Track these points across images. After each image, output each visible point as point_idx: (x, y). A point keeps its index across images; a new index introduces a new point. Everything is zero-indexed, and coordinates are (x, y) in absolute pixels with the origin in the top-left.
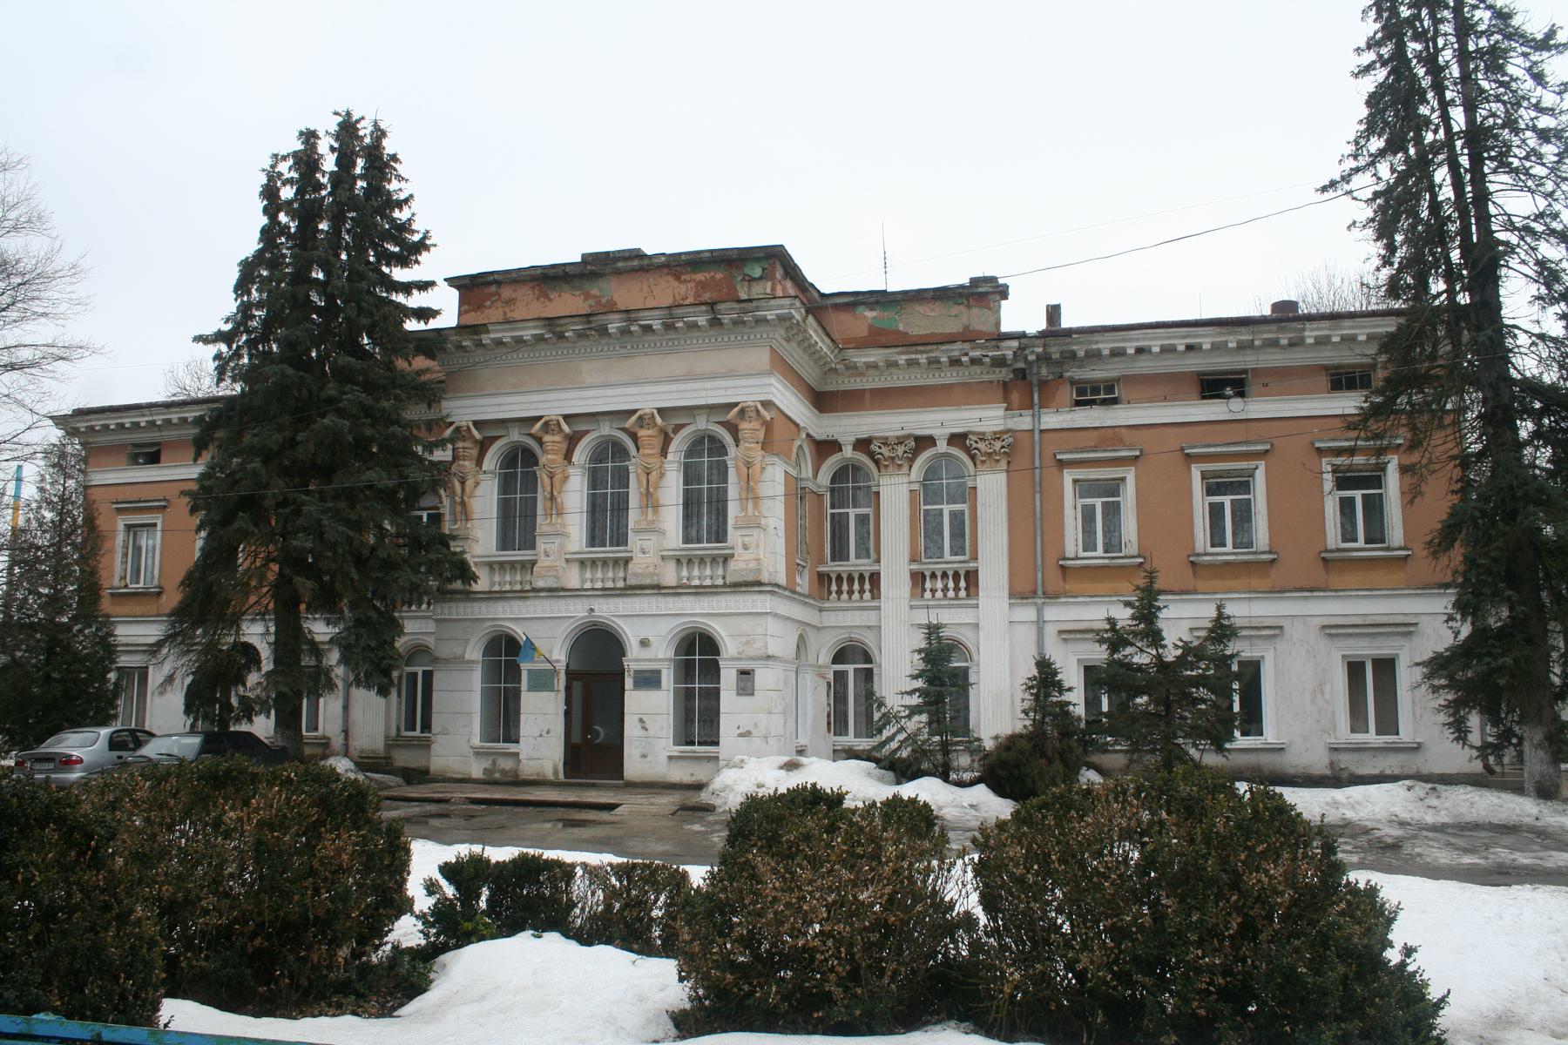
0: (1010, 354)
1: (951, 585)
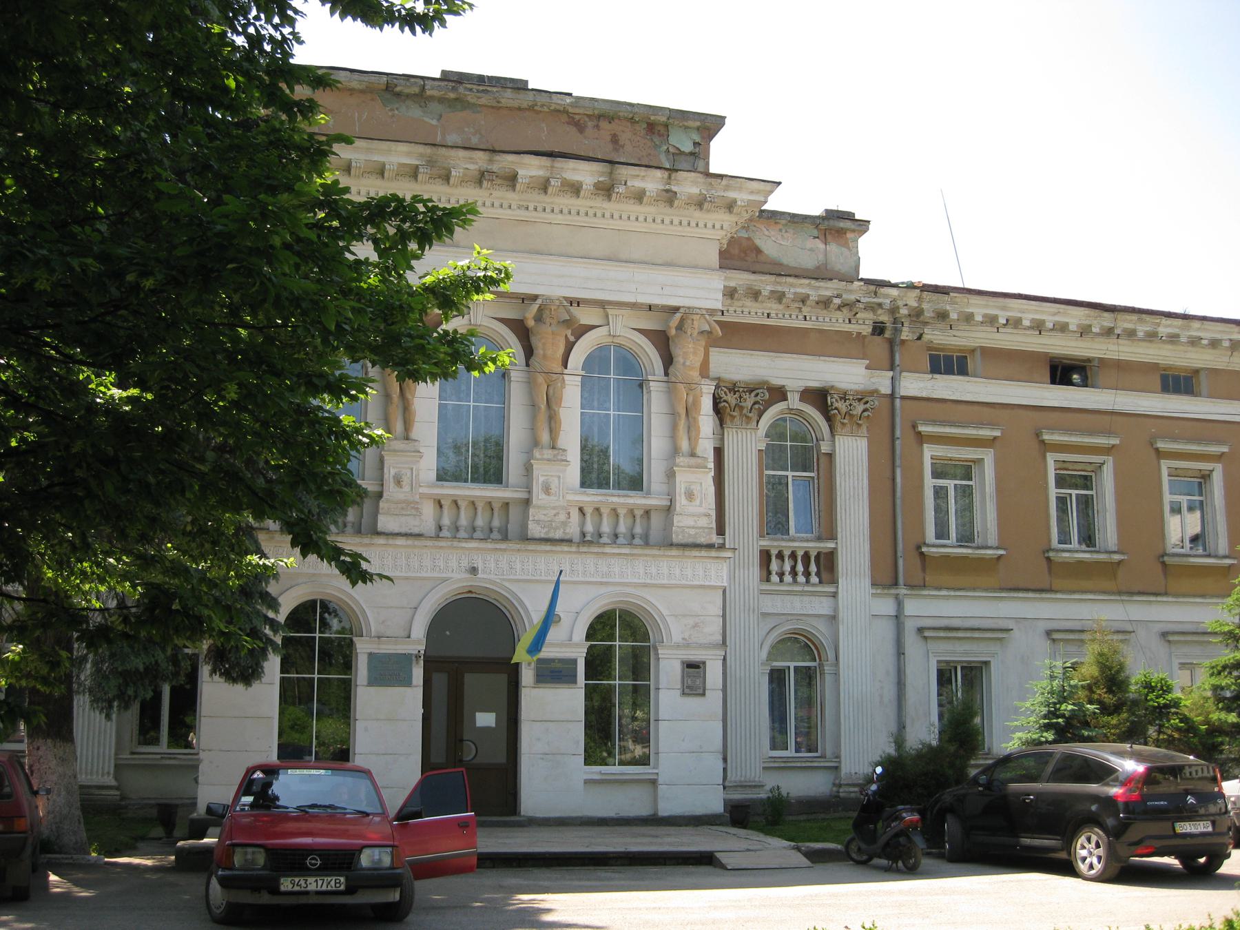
0: (887, 302)
1: (800, 568)
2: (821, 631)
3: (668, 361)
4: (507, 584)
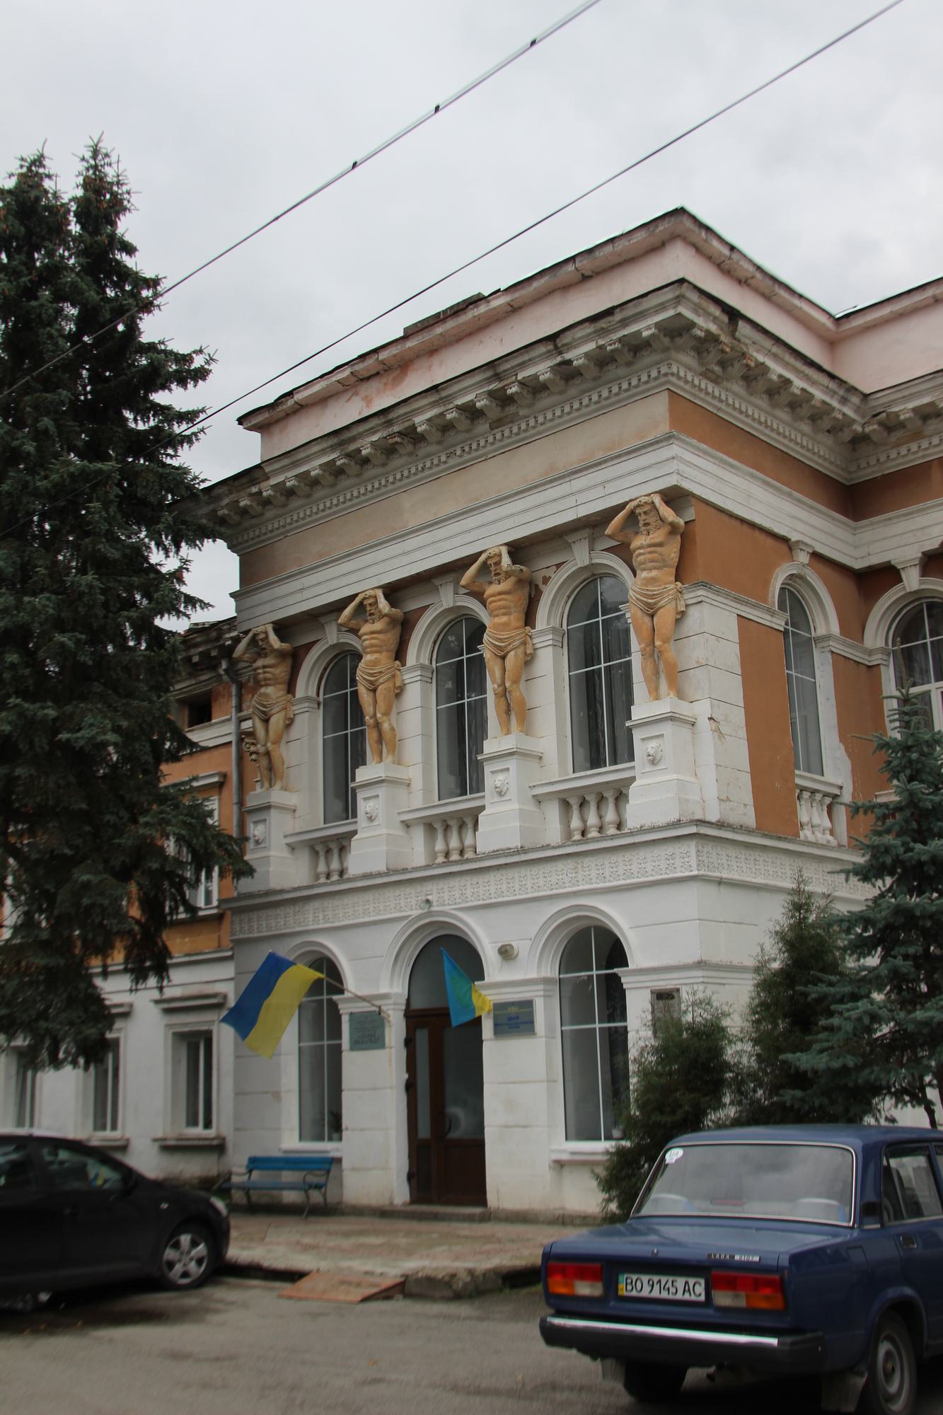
4: (460, 914)
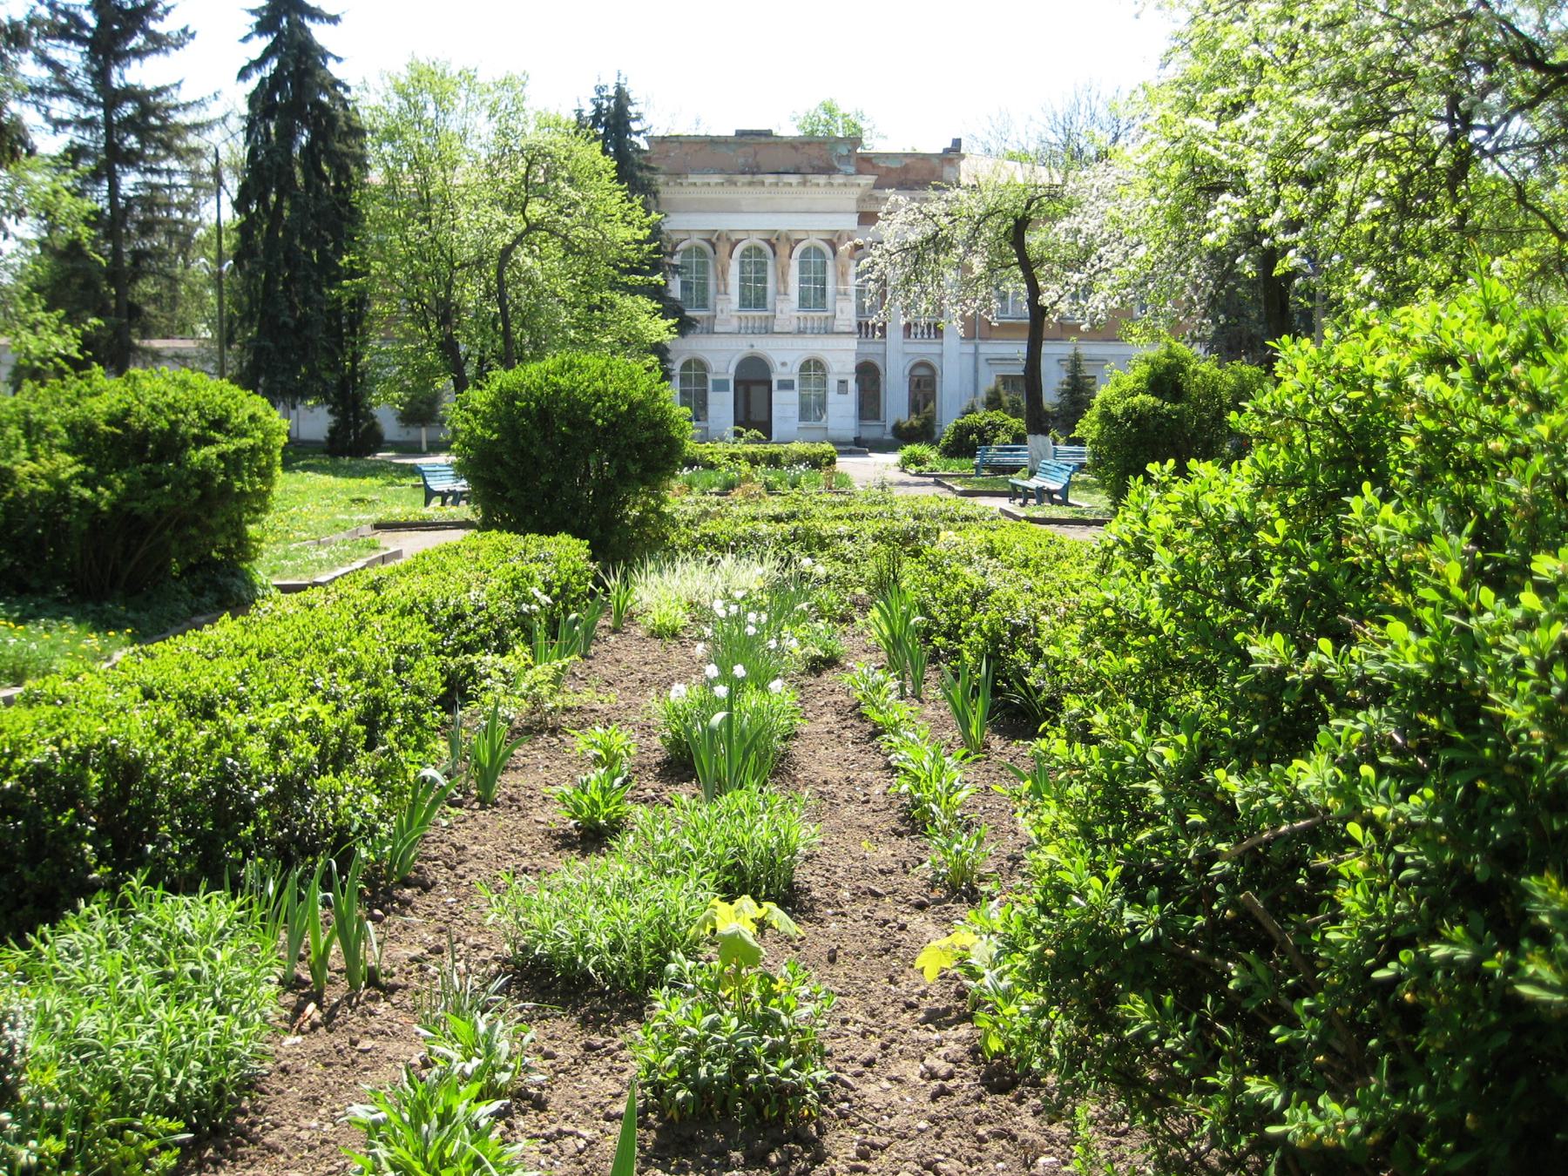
2: (935, 362)
3: (835, 253)
